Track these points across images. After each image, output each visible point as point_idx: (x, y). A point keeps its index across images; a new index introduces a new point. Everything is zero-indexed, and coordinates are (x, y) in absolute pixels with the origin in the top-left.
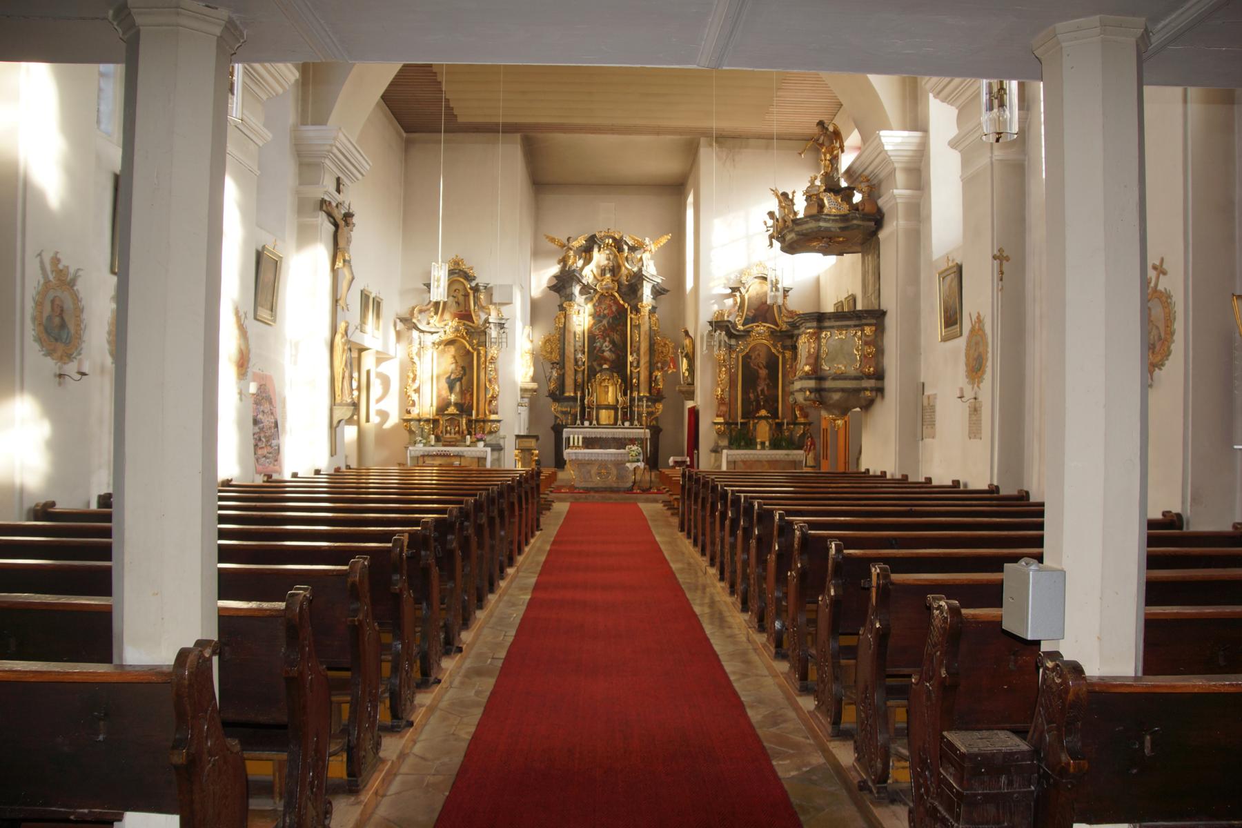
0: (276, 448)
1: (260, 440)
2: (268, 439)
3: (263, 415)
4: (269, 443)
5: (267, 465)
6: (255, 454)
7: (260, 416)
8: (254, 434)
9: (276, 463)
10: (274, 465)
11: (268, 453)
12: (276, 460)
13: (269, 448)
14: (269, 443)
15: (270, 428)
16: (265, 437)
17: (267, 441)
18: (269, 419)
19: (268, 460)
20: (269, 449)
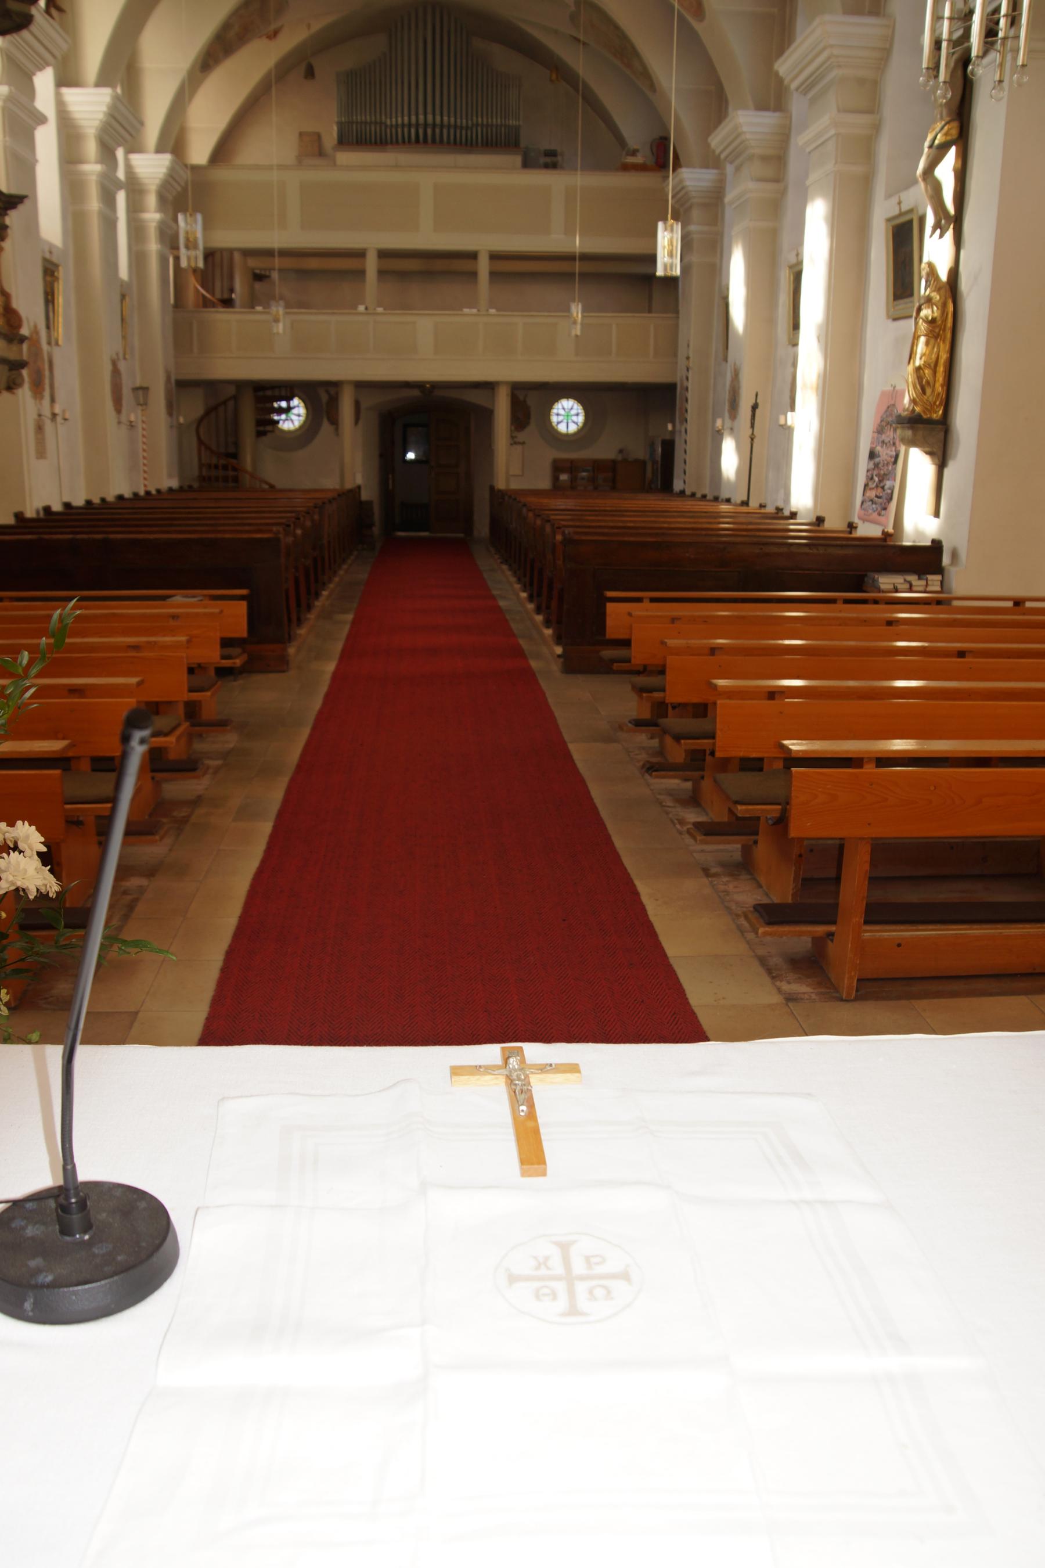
0: (889, 491)
1: (872, 478)
2: (882, 478)
3: (882, 447)
4: (882, 485)
5: (870, 511)
6: (864, 495)
7: (878, 448)
8: (868, 471)
9: (883, 512)
10: (879, 514)
11: (877, 496)
12: (885, 509)
13: (880, 490)
14: (882, 485)
15: (888, 464)
16: (878, 475)
17: (880, 481)
18: (889, 452)
19: (874, 506)
20: (879, 492)
